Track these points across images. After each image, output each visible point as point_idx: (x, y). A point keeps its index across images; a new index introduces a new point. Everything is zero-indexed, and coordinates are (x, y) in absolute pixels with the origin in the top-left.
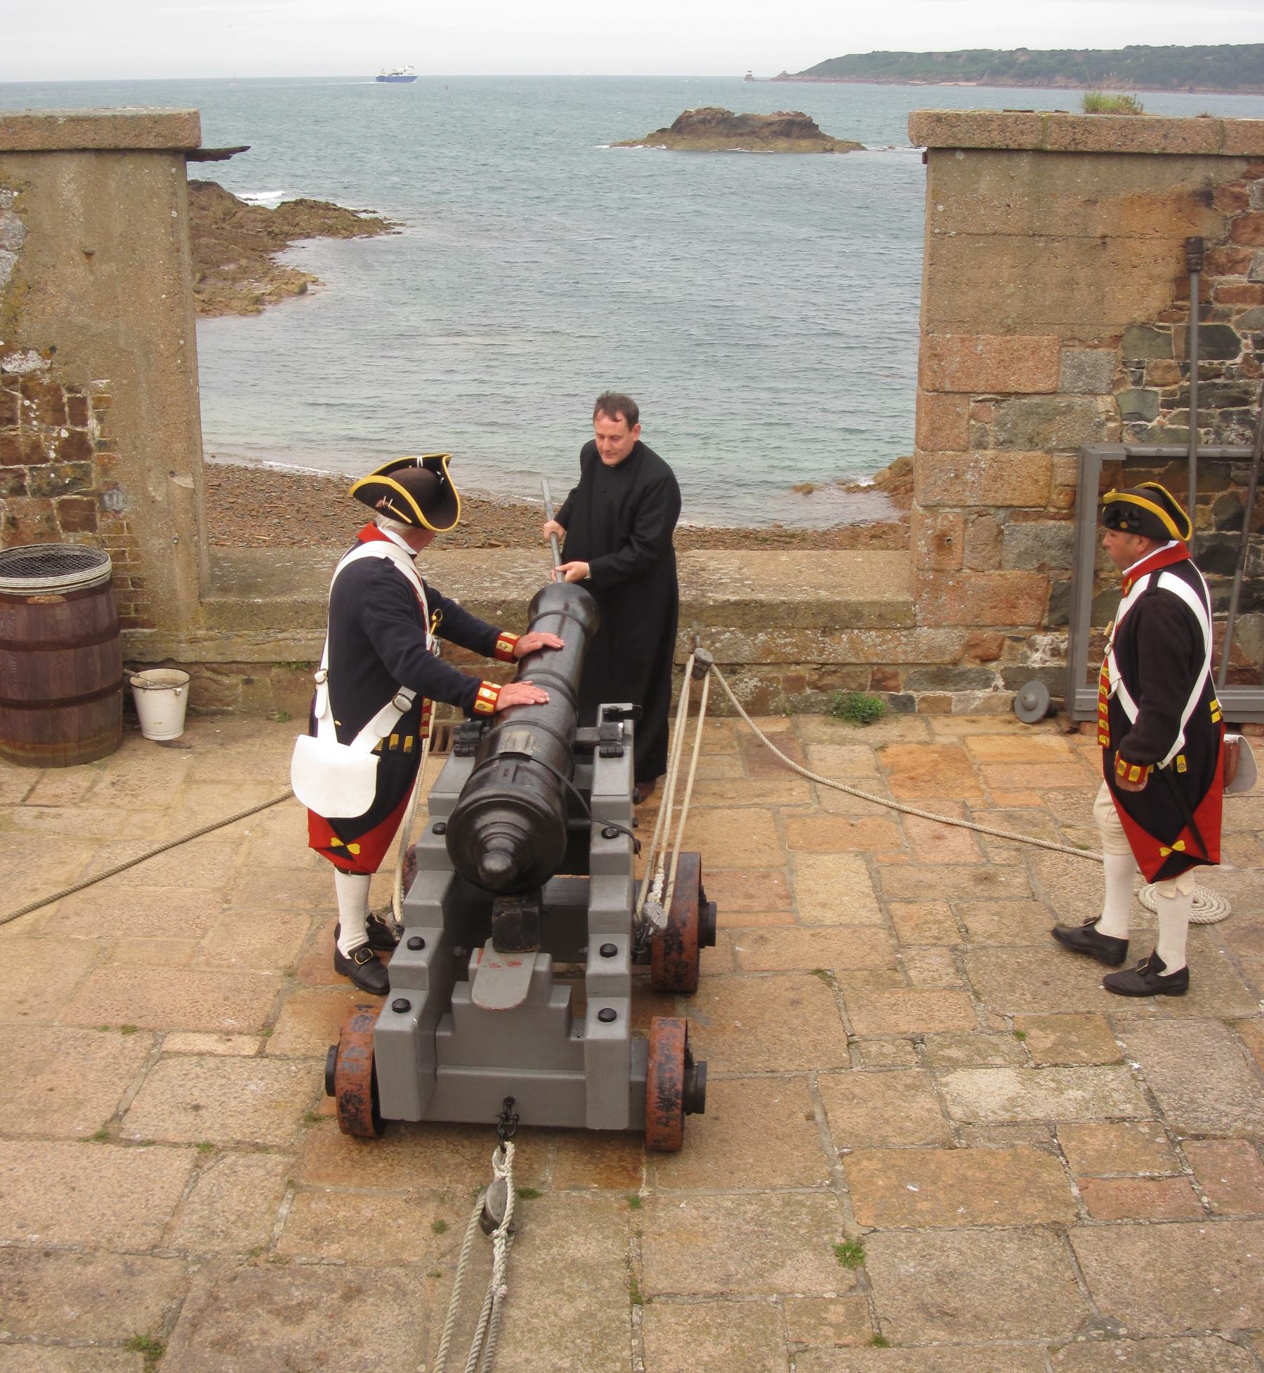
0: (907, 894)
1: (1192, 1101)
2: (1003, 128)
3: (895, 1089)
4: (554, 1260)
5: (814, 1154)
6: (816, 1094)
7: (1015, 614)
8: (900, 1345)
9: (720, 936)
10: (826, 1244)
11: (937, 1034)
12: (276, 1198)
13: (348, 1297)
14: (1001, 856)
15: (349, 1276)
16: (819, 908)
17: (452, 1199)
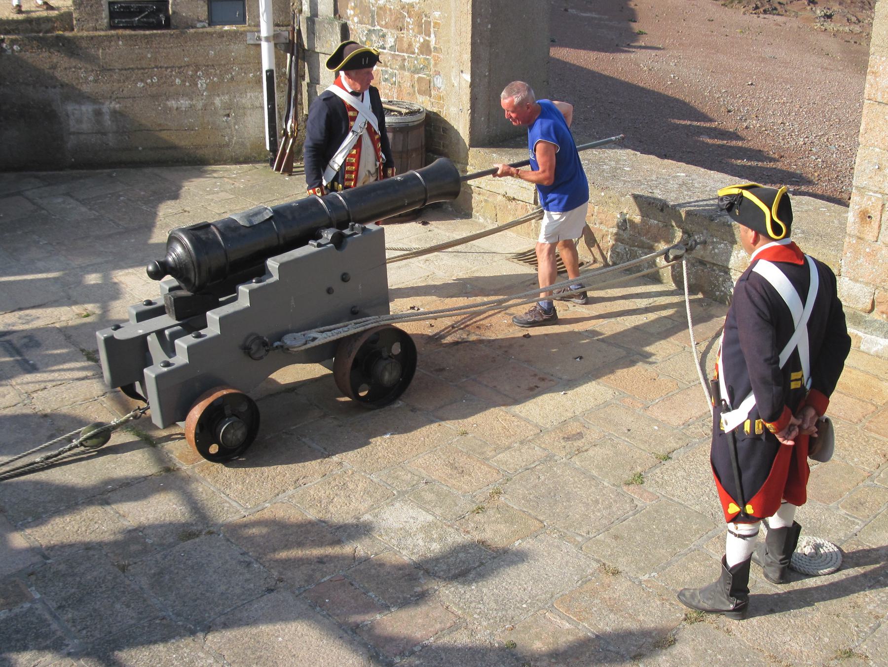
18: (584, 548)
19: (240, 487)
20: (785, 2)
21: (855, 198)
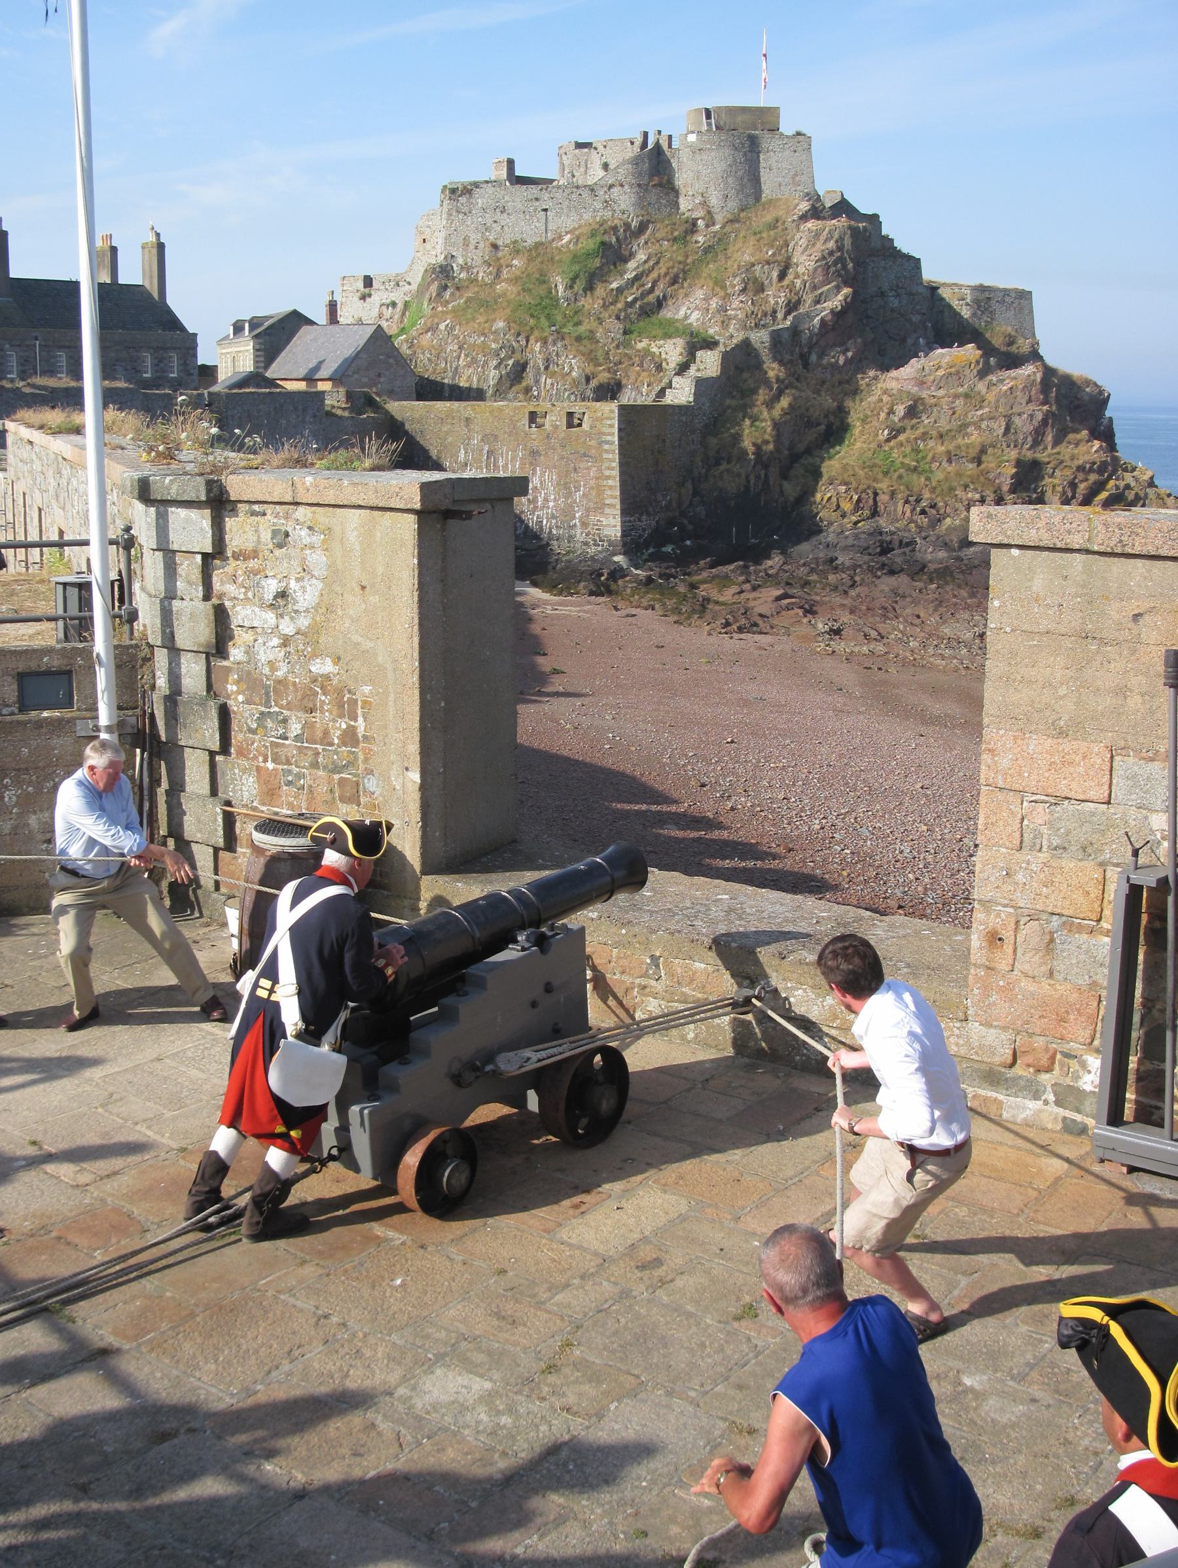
7: (1065, 1028)
18: (702, 1405)
19: (213, 1367)
20: (769, 614)
21: (979, 915)
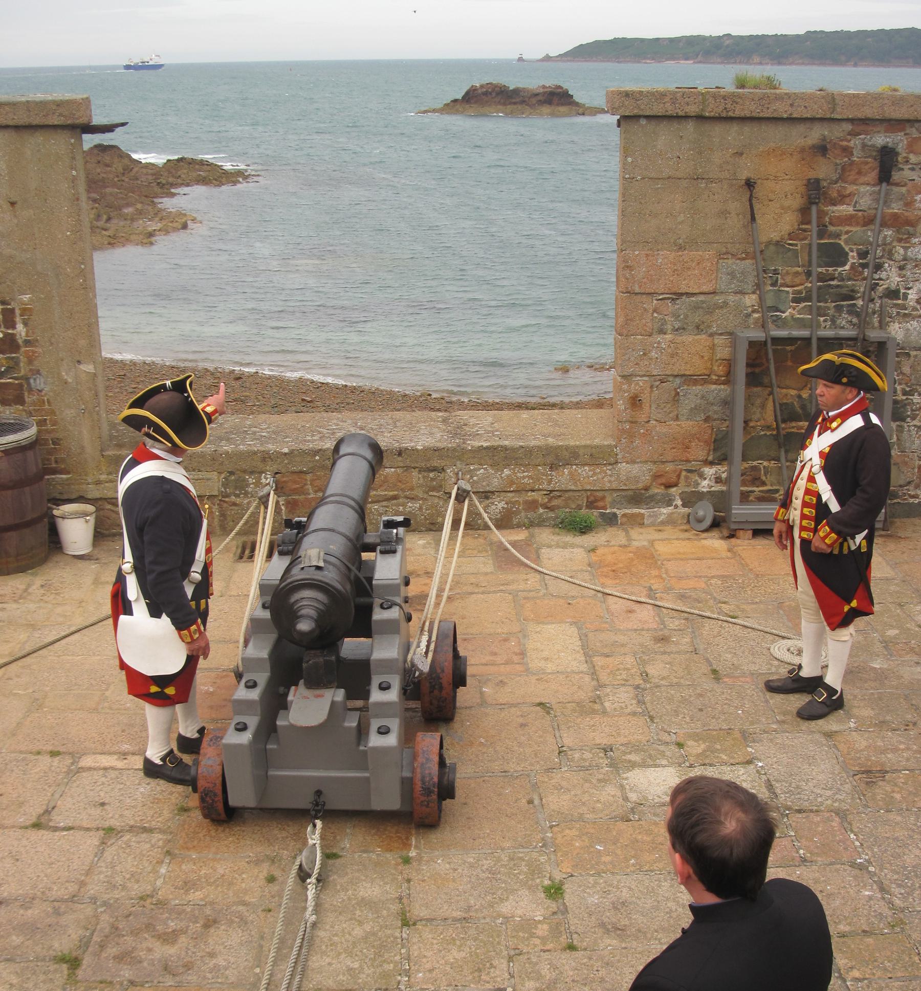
0: (606, 651)
1: (798, 787)
2: (674, 101)
3: (591, 782)
4: (349, 899)
5: (532, 826)
6: (535, 786)
8: (585, 949)
9: (469, 680)
10: (537, 885)
11: (622, 745)
12: (157, 862)
13: (207, 926)
14: (674, 624)
15: (208, 912)
16: (543, 661)
17: (280, 861)
